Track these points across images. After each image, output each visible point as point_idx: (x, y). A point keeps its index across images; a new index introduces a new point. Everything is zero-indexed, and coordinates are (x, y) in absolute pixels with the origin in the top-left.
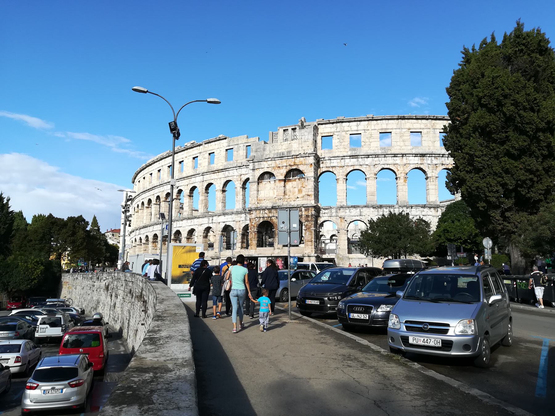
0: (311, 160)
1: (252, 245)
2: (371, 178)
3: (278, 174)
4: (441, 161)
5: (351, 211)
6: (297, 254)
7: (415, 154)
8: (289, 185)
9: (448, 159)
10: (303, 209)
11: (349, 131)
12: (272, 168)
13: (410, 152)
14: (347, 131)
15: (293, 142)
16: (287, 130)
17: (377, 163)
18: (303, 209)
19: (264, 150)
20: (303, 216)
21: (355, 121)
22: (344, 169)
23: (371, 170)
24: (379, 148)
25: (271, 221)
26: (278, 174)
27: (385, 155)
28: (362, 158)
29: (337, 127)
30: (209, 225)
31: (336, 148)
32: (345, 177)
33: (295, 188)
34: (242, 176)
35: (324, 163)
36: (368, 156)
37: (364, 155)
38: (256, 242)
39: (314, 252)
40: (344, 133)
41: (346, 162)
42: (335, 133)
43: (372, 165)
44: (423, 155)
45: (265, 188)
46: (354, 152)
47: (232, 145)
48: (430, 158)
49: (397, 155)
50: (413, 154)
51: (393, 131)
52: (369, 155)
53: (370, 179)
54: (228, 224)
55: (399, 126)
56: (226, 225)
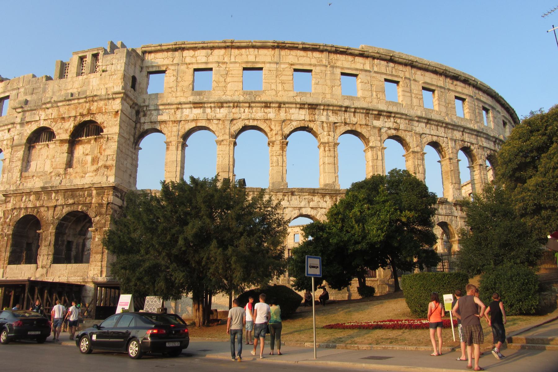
0: (117, 105)
2: (225, 142)
4: (343, 118)
6: (73, 278)
7: (301, 104)
8: (79, 150)
9: (354, 116)
10: (94, 192)
11: (192, 63)
13: (292, 100)
14: (189, 64)
15: (92, 75)
16: (85, 57)
17: (237, 116)
18: (94, 192)
19: (44, 91)
20: (93, 206)
21: (203, 48)
22: (180, 126)
23: (224, 128)
24: (241, 92)
25: (37, 216)
27: (249, 103)
28: (211, 107)
29: (173, 58)
31: (170, 90)
32: (182, 140)
35: (148, 116)
36: (221, 104)
37: (214, 103)
39: (104, 275)
40: (183, 67)
41: (185, 113)
42: (170, 67)
43: (228, 120)
44: (313, 107)
45: (39, 156)
46: (198, 97)
47: (9, 91)
48: (325, 113)
49: (270, 103)
50: (296, 104)
51: (266, 67)
52: (222, 103)
53: (222, 143)
55: (276, 59)
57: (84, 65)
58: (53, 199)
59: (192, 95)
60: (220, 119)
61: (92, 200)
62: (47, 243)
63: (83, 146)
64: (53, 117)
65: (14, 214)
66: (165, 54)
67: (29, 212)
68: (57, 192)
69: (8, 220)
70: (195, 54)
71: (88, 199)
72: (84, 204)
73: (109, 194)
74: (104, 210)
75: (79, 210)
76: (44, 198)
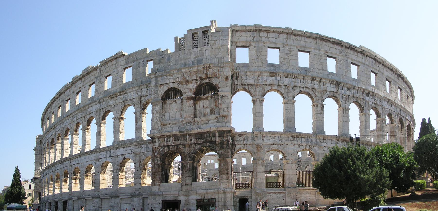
1: (155, 180)
8: (200, 104)
10: (217, 134)
18: (217, 134)
33: (207, 108)
34: (143, 98)
38: (160, 176)
45: (170, 109)
54: (126, 156)
58: (187, 139)
61: (216, 139)
63: (202, 101)
65: (159, 150)
66: (248, 34)
68: (190, 135)
69: (156, 154)
72: (211, 142)
75: (207, 146)
76: (181, 139)
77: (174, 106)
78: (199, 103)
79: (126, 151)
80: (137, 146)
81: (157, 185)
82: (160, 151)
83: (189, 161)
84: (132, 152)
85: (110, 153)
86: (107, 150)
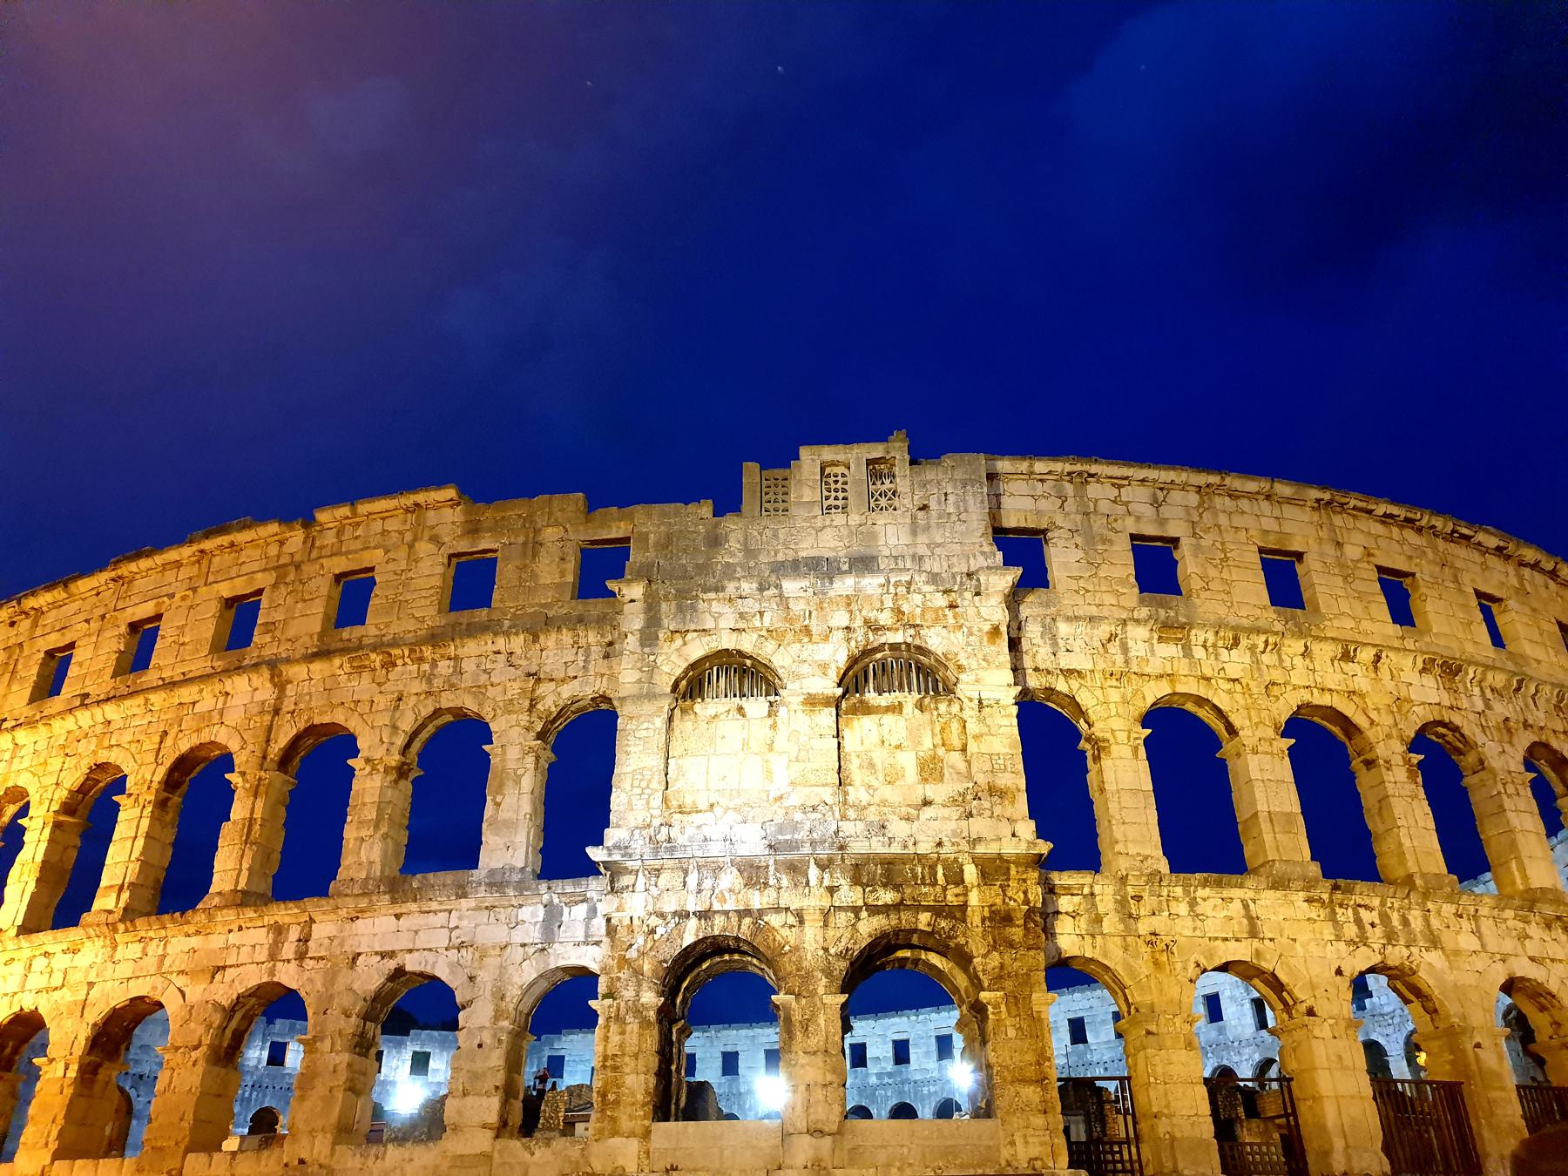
3: (805, 669)
5: (1199, 909)
10: (971, 873)
12: (764, 633)
18: (971, 873)
20: (975, 918)
26: (805, 669)
30: (272, 972)
33: (899, 747)
34: (545, 688)
54: (412, 964)
56: (399, 972)
57: (833, 486)
58: (813, 882)
59: (1142, 602)
60: (1234, 680)
61: (966, 895)
62: (815, 1042)
64: (767, 623)
65: (653, 931)
67: (718, 926)
70: (1120, 495)
71: (952, 891)
72: (938, 911)
73: (1025, 881)
74: (1016, 933)
75: (922, 926)
77: (731, 728)
78: (861, 726)
79: (416, 932)
80: (487, 908)
81: (632, 1134)
82: (657, 937)
83: (828, 999)
84: (456, 942)
85: (305, 940)
86: (287, 920)
